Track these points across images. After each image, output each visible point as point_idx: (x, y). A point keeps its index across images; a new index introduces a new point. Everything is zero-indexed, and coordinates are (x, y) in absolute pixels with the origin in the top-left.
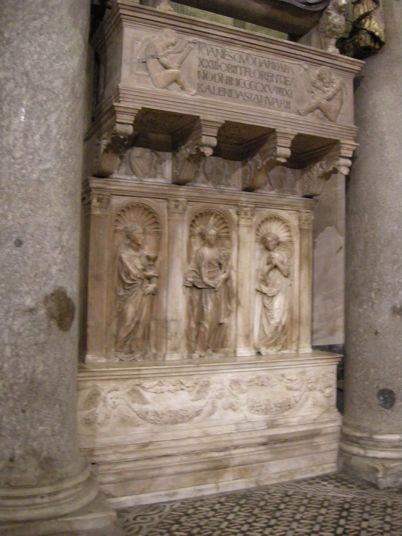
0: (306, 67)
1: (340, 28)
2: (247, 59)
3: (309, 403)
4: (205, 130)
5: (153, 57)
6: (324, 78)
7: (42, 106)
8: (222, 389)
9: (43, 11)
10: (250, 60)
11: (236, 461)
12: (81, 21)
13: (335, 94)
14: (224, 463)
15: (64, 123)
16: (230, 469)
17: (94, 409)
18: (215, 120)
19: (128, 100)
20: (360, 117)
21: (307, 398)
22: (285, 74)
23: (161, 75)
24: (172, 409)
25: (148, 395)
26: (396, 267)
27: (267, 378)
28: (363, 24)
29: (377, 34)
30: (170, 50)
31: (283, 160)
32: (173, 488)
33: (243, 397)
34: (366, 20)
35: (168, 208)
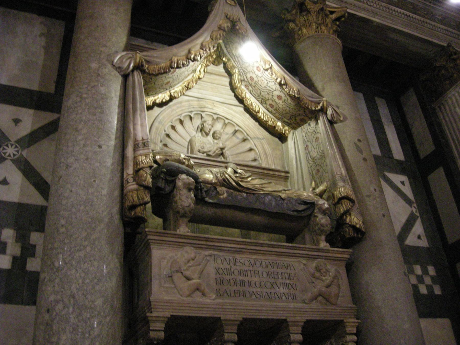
0: (304, 262)
1: (327, 226)
4: (226, 328)
5: (177, 271)
6: (321, 270)
7: (86, 323)
9: (86, 243)
10: (258, 263)
12: (117, 248)
13: (333, 281)
15: (105, 335)
18: (235, 319)
19: (158, 310)
20: (358, 296)
22: (289, 271)
23: (184, 285)
28: (346, 220)
29: (358, 226)
30: (190, 265)
34: (346, 217)
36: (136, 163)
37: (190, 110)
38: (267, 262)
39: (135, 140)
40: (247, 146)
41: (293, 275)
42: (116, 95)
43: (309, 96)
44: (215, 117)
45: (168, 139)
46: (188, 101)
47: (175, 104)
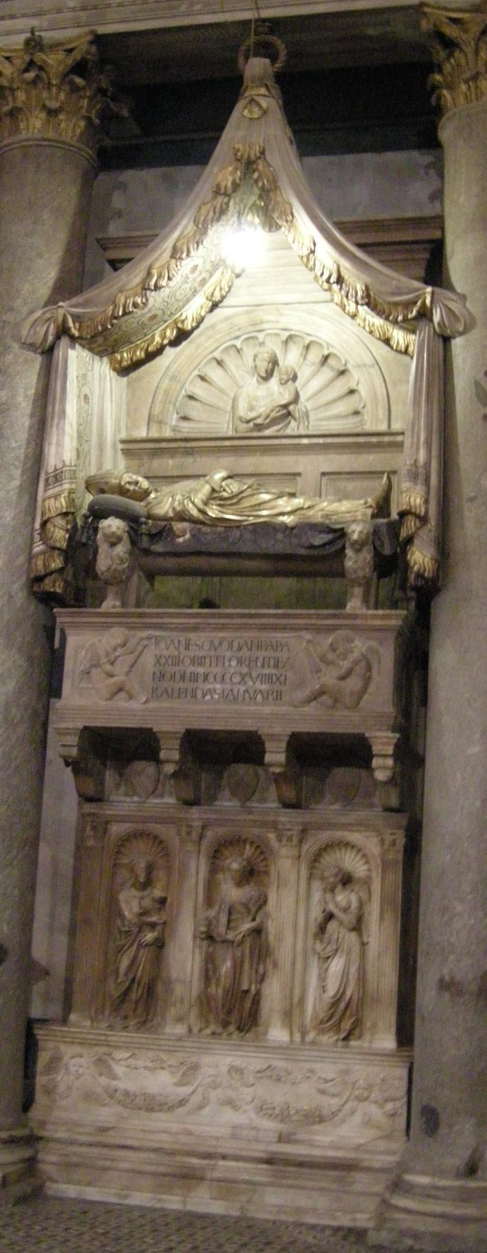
0: (307, 636)
1: (356, 572)
2: (221, 643)
3: (357, 1118)
5: (97, 665)
10: (225, 644)
11: (216, 1174)
16: (206, 1183)
21: (353, 1112)
22: (276, 654)
25: (119, 1069)
31: (278, 770)
32: (127, 1188)
33: (247, 1093)
36: (43, 514)
37: (233, 335)
39: (47, 473)
40: (341, 386)
42: (26, 396)
43: (393, 294)
44: (285, 335)
45: (193, 403)
46: (227, 318)
47: (207, 328)
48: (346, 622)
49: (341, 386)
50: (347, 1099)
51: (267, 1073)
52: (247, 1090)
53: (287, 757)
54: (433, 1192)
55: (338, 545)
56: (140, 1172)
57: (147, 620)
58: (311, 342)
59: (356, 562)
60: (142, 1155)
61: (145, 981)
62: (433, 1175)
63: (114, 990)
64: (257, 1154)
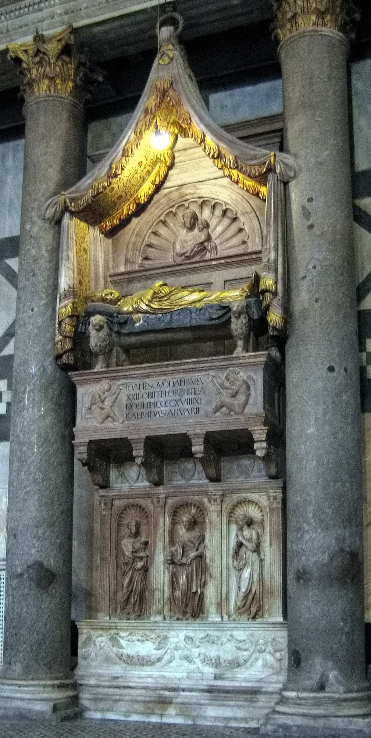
2: (163, 383)
3: (260, 663)
8: (177, 643)
10: (166, 384)
11: (179, 700)
14: (169, 700)
16: (173, 705)
17: (88, 648)
21: (257, 659)
22: (196, 386)
24: (140, 654)
25: (123, 642)
26: (299, 535)
27: (217, 637)
30: (106, 396)
33: (195, 652)
35: (153, 503)
38: (175, 380)
39: (60, 294)
40: (234, 228)
41: (200, 389)
48: (234, 362)
49: (234, 228)
50: (251, 652)
51: (209, 640)
52: (194, 650)
53: (204, 447)
54: (298, 701)
55: (227, 317)
56: (137, 701)
57: (121, 374)
58: (216, 203)
59: (238, 325)
60: (139, 691)
61: (138, 591)
62: (298, 691)
63: (121, 597)
64: (202, 687)
